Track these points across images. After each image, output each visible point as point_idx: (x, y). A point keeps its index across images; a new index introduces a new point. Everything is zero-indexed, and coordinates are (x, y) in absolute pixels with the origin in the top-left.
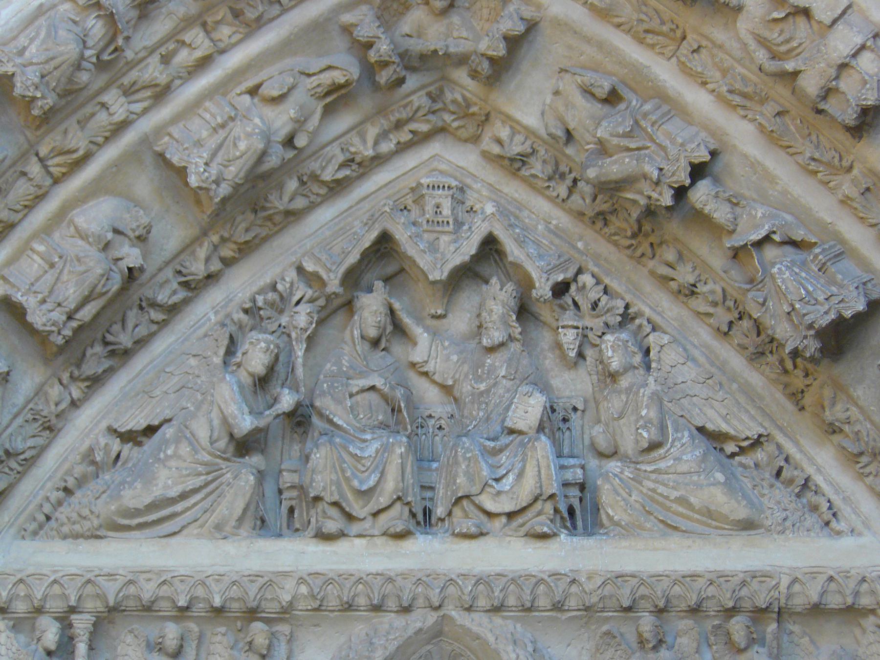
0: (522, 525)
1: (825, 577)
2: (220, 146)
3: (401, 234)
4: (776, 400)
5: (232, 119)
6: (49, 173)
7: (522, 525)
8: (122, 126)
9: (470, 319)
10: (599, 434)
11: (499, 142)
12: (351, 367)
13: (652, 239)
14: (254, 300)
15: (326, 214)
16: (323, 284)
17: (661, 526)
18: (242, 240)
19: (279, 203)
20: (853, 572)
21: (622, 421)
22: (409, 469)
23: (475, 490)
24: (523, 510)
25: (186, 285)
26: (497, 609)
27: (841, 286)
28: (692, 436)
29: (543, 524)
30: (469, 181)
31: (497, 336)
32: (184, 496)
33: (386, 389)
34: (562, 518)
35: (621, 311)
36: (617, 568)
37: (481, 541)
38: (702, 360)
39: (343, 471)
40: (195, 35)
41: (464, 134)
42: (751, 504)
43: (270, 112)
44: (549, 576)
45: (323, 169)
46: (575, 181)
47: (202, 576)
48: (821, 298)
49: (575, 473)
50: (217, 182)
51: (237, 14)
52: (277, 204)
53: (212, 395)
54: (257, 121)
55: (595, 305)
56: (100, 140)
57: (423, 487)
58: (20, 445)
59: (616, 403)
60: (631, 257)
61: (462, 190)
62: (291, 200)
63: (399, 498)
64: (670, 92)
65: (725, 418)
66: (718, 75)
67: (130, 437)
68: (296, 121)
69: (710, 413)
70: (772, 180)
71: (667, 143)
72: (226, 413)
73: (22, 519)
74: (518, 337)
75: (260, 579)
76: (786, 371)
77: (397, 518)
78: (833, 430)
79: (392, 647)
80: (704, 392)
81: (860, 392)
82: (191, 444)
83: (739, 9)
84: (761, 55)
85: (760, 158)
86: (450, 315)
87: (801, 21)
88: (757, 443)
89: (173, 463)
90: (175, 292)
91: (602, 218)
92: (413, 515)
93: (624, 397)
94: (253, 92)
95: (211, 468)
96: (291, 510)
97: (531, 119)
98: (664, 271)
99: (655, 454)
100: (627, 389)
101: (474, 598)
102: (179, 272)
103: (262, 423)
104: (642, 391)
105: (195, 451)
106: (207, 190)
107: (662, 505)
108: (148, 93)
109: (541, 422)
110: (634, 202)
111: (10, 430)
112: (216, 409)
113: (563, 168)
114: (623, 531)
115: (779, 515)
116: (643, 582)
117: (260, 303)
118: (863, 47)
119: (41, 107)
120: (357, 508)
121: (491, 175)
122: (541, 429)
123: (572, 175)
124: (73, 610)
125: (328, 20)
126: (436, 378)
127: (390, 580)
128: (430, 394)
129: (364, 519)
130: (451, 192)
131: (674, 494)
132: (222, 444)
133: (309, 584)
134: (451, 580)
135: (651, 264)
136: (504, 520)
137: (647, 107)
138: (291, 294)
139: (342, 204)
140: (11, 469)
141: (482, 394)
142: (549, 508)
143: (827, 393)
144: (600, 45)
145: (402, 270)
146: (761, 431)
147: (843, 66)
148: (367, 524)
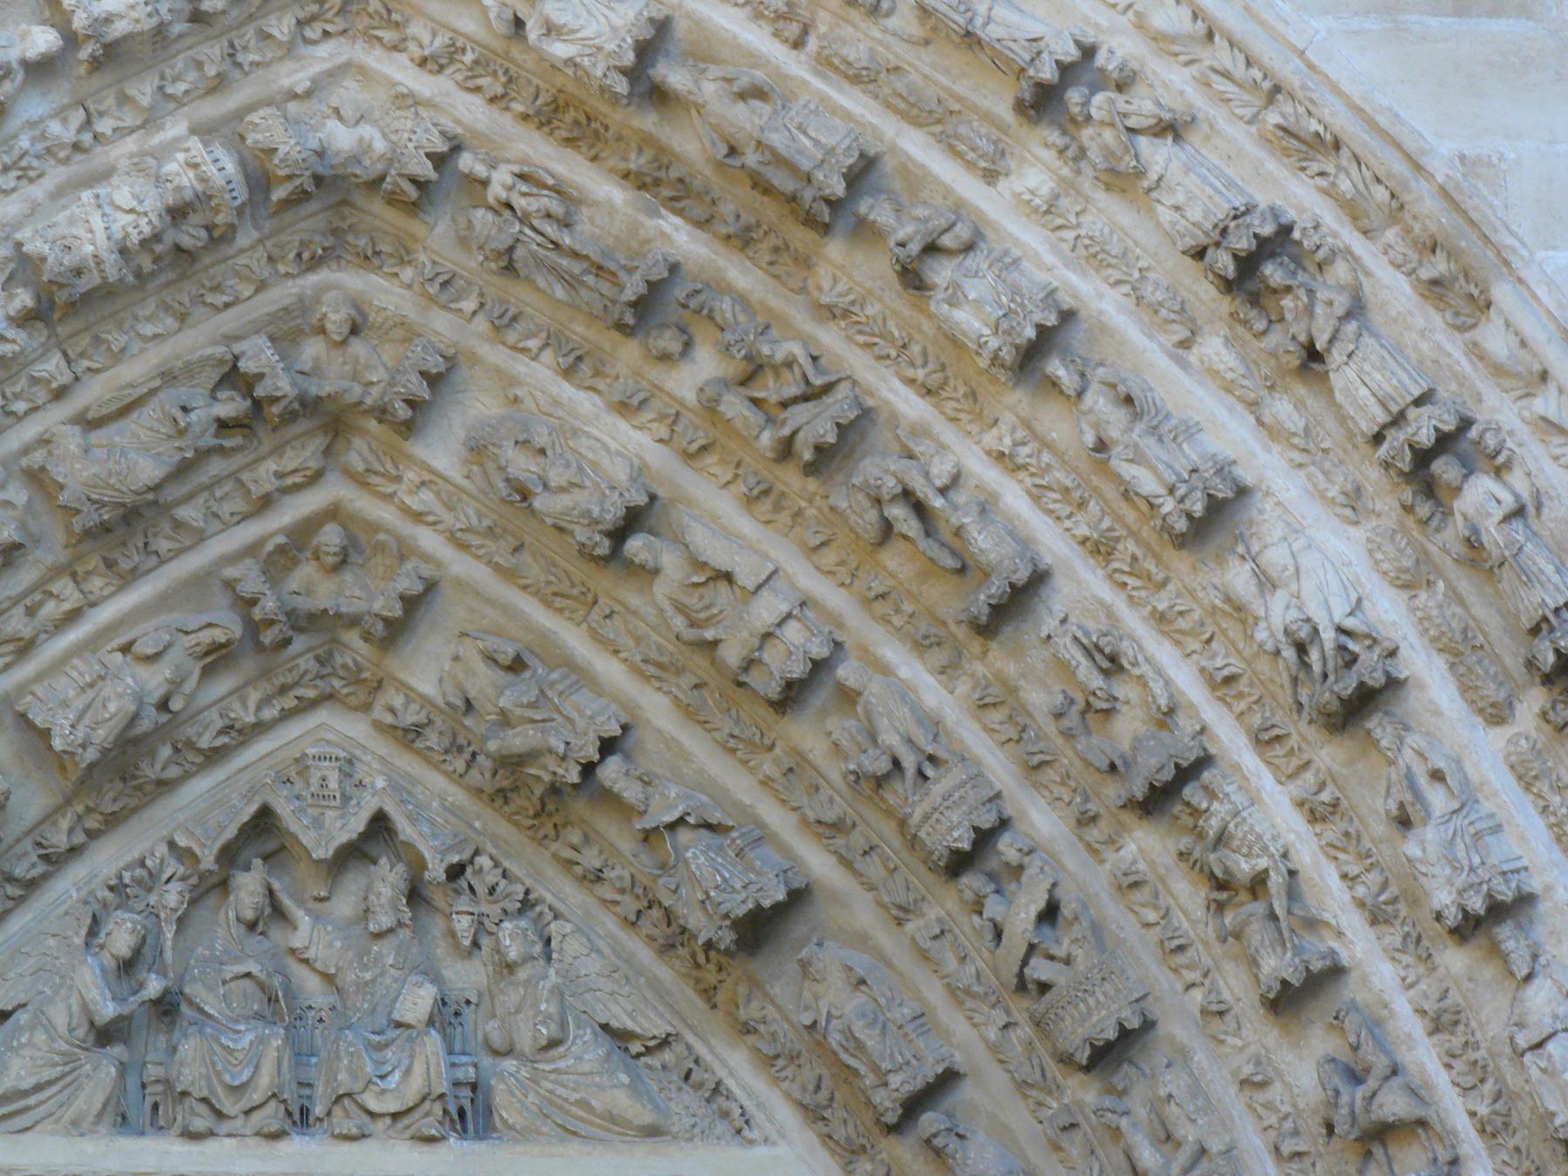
0: (408, 1127)
2: (88, 707)
4: (686, 995)
5: (102, 678)
7: (408, 1127)
10: (493, 1029)
11: (392, 711)
12: (225, 951)
13: (557, 819)
14: (120, 877)
15: (201, 785)
16: (196, 859)
18: (109, 810)
19: (150, 771)
21: (519, 1017)
22: (285, 1063)
23: (357, 1087)
24: (409, 1110)
25: (45, 858)
27: (759, 874)
28: (595, 1034)
29: (431, 1127)
30: (358, 753)
31: (385, 920)
32: (38, 1088)
33: (263, 977)
34: (452, 1120)
35: (521, 896)
38: (607, 951)
39: (214, 1064)
40: (64, 586)
41: (353, 700)
42: (657, 1108)
43: (143, 672)
45: (200, 735)
46: (474, 755)
48: (738, 886)
50: (84, 746)
51: (110, 564)
54: (129, 680)
55: (492, 890)
57: (300, 1084)
59: (512, 997)
60: (533, 839)
61: (350, 762)
62: (164, 768)
63: (274, 1095)
65: (630, 1015)
66: (631, 643)
68: (172, 682)
69: (615, 1008)
70: (687, 757)
71: (575, 715)
76: (698, 966)
77: (270, 1117)
78: (747, 1029)
80: (608, 986)
81: (777, 990)
82: (47, 1031)
83: (656, 572)
84: (679, 622)
86: (334, 898)
87: (723, 586)
88: (665, 1043)
89: (27, 1052)
90: (33, 866)
91: (502, 796)
92: (289, 1114)
93: (522, 990)
94: (126, 649)
95: (69, 1059)
96: (155, 1107)
97: (427, 686)
98: (568, 853)
99: (554, 1052)
102: (39, 844)
103: (126, 1010)
105: (51, 1038)
106: (73, 754)
107: (561, 1108)
108: (10, 647)
109: (431, 1015)
110: (538, 778)
112: (75, 993)
113: (461, 740)
115: (688, 1122)
117: (127, 881)
118: (789, 616)
121: (382, 747)
122: (430, 1022)
125: (209, 574)
126: (318, 965)
128: (310, 983)
131: (575, 1096)
132: (81, 1032)
135: (554, 846)
136: (388, 1121)
137: (555, 676)
138: (161, 871)
139: (219, 774)
141: (367, 983)
142: (437, 1109)
143: (742, 990)
144: (505, 609)
145: (283, 848)
146: (670, 1029)
147: (767, 636)
148: (239, 1123)
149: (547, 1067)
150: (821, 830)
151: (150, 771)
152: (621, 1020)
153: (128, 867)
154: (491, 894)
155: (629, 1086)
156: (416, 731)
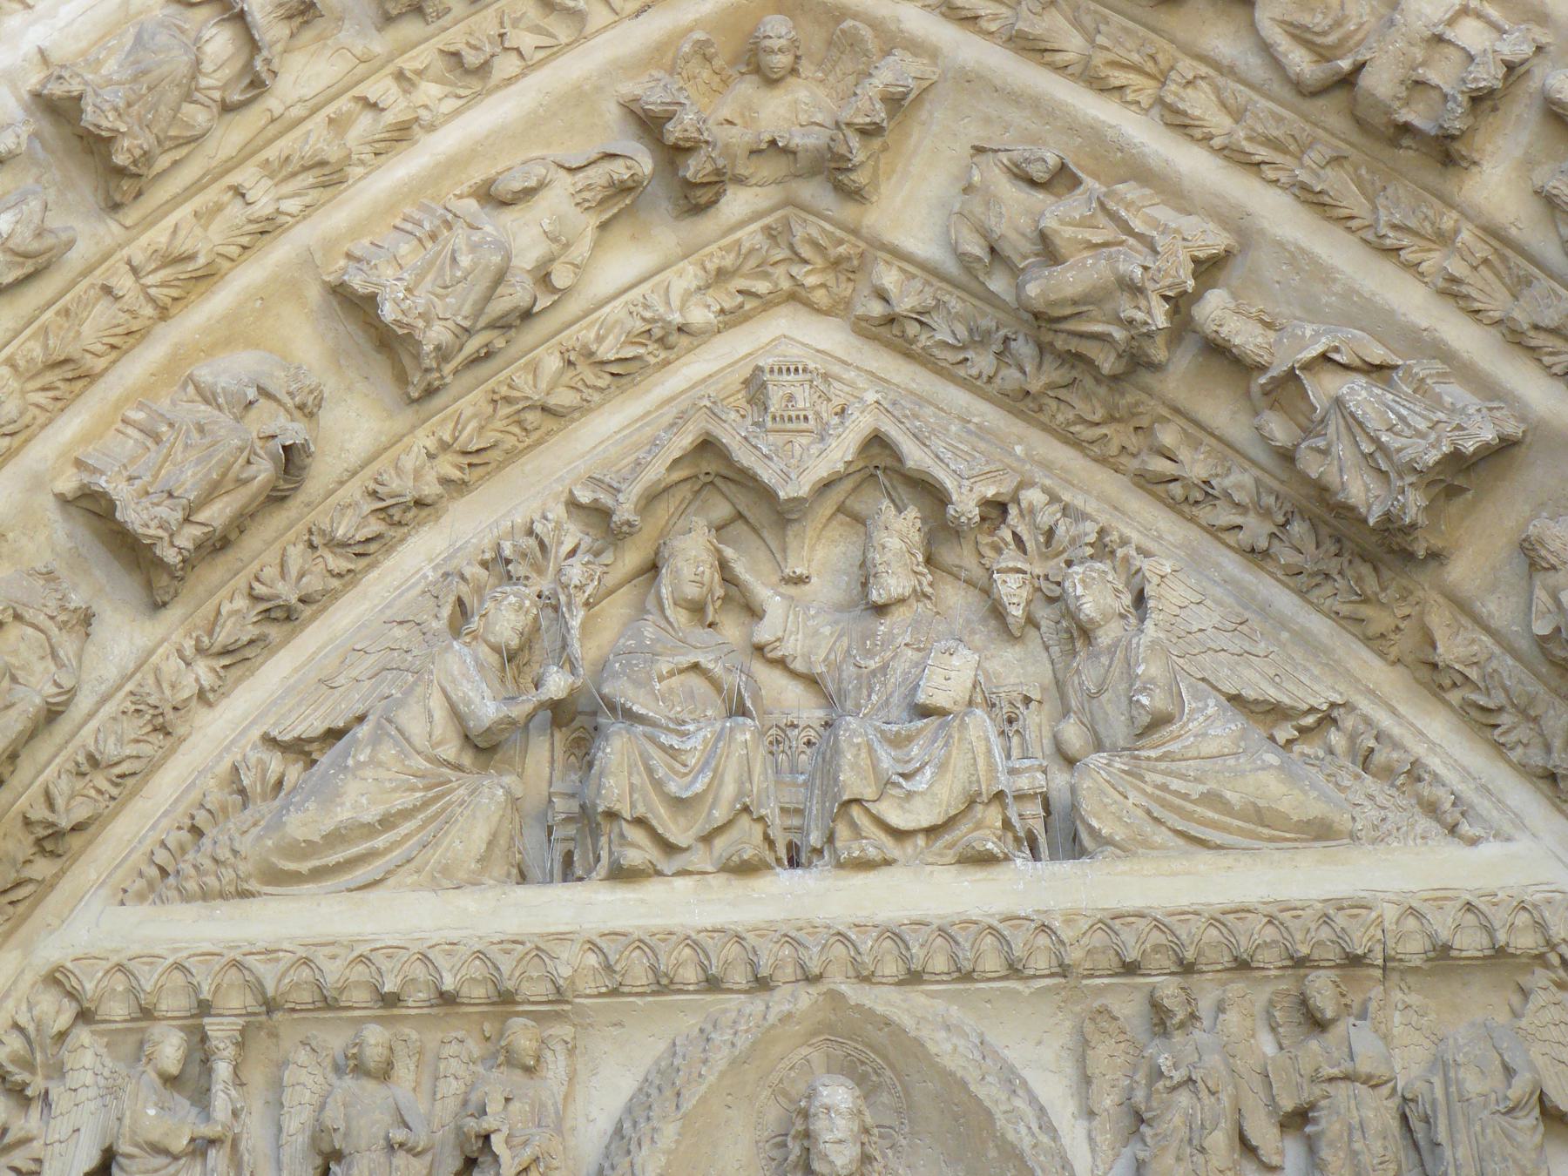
1: (1458, 904)
6: (151, 300)
7: (950, 846)
8: (267, 229)
9: (848, 584)
11: (883, 296)
17: (1181, 842)
20: (1501, 895)
23: (869, 793)
24: (949, 823)
26: (914, 977)
30: (836, 369)
32: (387, 822)
33: (717, 669)
35: (1092, 538)
36: (1113, 903)
39: (650, 771)
44: (1001, 921)
45: (600, 339)
47: (423, 947)
48: (1422, 425)
49: (1034, 778)
53: (431, 672)
56: (233, 251)
58: (111, 750)
59: (1088, 673)
63: (746, 809)
64: (1154, 163)
67: (299, 749)
69: (1249, 674)
70: (1326, 275)
72: (454, 697)
73: (120, 873)
75: (519, 947)
79: (743, 1043)
82: (396, 744)
84: (1300, 61)
85: (1305, 242)
88: (1328, 719)
89: (369, 773)
98: (1161, 465)
100: (1109, 646)
101: (877, 961)
102: (374, 494)
104: (1135, 641)
107: (1179, 811)
108: (309, 178)
111: (94, 724)
114: (1118, 852)
115: (1374, 814)
116: (1159, 925)
117: (508, 551)
119: (129, 150)
120: (677, 833)
123: (1002, 332)
124: (204, 1008)
125: (599, 89)
126: (798, 666)
130: (808, 376)
131: (1196, 790)
132: (450, 750)
133: (601, 950)
134: (839, 934)
140: (100, 792)
142: (993, 816)
144: (1037, 105)
149: (1153, 754)
150: (1538, 340)
152: (1257, 686)
154: (1048, 543)
155: (1280, 768)
156: (921, 318)
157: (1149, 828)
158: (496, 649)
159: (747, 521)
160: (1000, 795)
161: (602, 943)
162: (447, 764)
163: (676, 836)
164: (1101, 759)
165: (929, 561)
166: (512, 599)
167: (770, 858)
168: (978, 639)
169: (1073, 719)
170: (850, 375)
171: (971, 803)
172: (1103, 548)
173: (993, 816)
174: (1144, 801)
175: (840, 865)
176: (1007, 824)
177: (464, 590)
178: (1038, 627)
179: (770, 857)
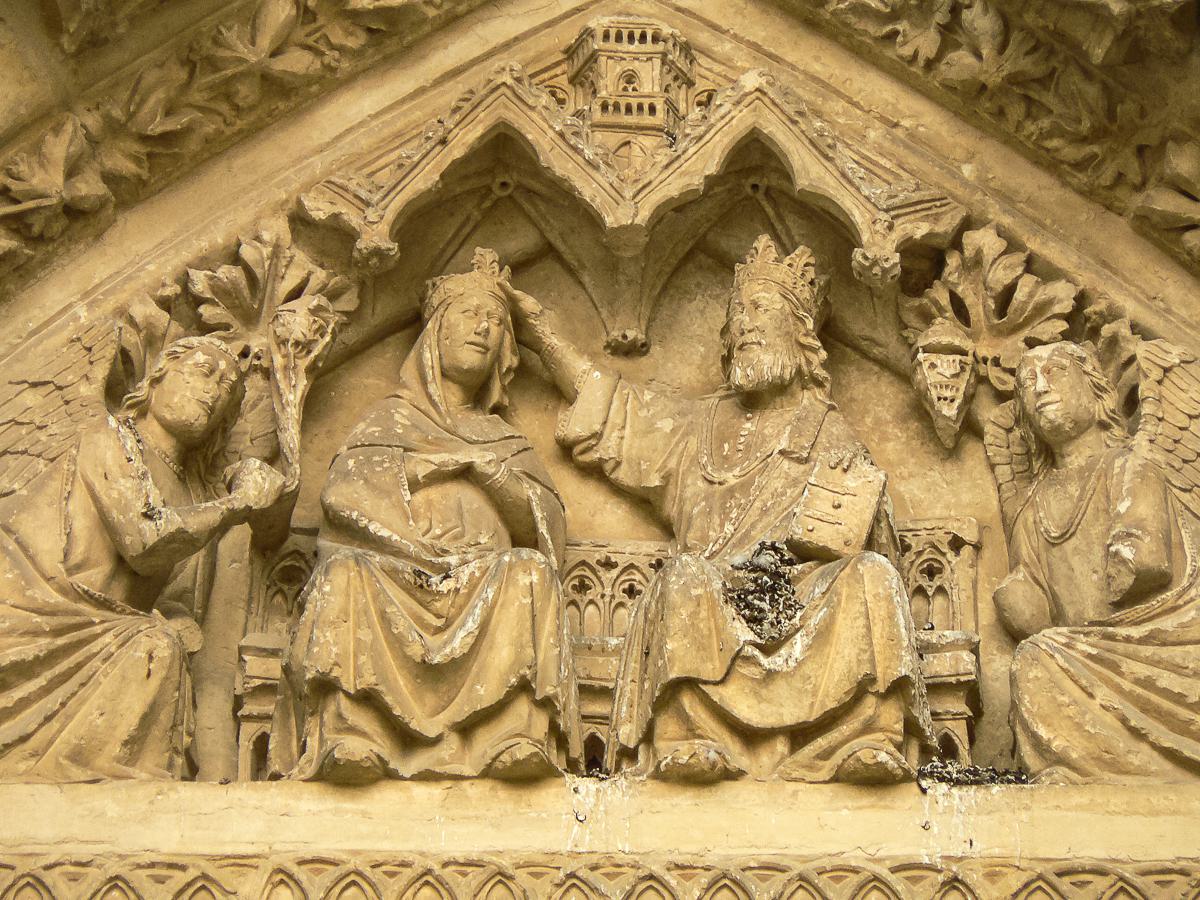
0: (826, 755)
3: (541, 131)
7: (826, 755)
9: (704, 358)
14: (184, 280)
17: (1168, 766)
18: (157, 128)
21: (1069, 546)
23: (711, 669)
24: (829, 721)
30: (704, 38)
31: (766, 362)
33: (500, 475)
35: (1066, 306)
37: (729, 789)
44: (894, 870)
47: (34, 865)
49: (958, 660)
52: (243, 50)
53: (73, 461)
59: (1052, 505)
60: (1088, 194)
63: (524, 687)
72: (105, 500)
74: (821, 373)
75: (177, 874)
82: (16, 563)
86: (656, 350)
99: (1155, 603)
100: (1081, 470)
104: (1118, 463)
112: (80, 495)
114: (1074, 776)
117: (200, 283)
122: (870, 544)
126: (624, 476)
127: (503, 877)
129: (437, 741)
130: (660, 47)
132: (94, 578)
133: (297, 883)
134: (651, 877)
136: (781, 746)
142: (891, 716)
149: (1136, 632)
151: (251, 52)
153: (203, 262)
157: (1122, 742)
158: (169, 428)
159: (559, 258)
160: (899, 687)
161: (300, 874)
162: (87, 597)
163: (425, 724)
164: (1052, 636)
165: (829, 331)
166: (200, 357)
167: (560, 763)
168: (892, 449)
169: (1021, 574)
170: (725, 47)
171: (862, 689)
172: (1080, 323)
173: (891, 716)
174: (1116, 702)
175: (659, 776)
176: (911, 728)
177: (132, 339)
178: (978, 434)
179: (558, 761)
